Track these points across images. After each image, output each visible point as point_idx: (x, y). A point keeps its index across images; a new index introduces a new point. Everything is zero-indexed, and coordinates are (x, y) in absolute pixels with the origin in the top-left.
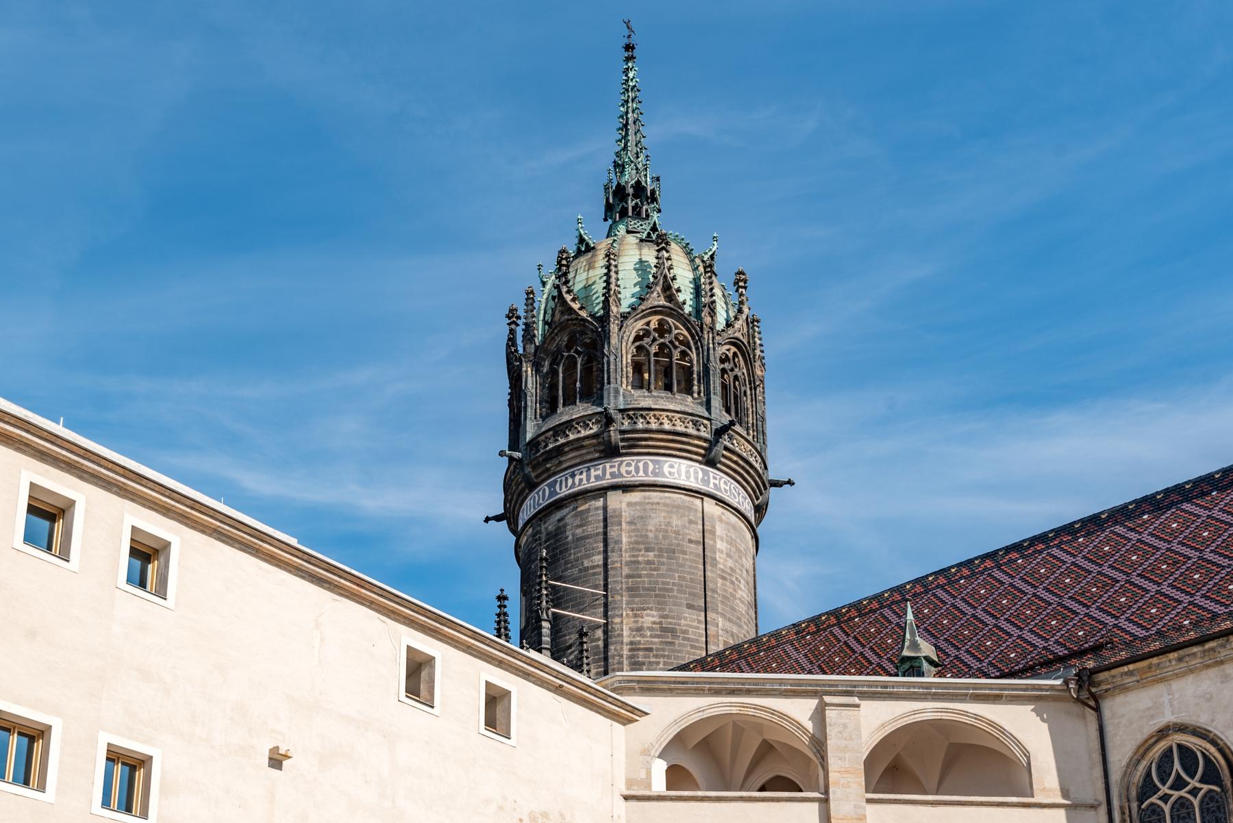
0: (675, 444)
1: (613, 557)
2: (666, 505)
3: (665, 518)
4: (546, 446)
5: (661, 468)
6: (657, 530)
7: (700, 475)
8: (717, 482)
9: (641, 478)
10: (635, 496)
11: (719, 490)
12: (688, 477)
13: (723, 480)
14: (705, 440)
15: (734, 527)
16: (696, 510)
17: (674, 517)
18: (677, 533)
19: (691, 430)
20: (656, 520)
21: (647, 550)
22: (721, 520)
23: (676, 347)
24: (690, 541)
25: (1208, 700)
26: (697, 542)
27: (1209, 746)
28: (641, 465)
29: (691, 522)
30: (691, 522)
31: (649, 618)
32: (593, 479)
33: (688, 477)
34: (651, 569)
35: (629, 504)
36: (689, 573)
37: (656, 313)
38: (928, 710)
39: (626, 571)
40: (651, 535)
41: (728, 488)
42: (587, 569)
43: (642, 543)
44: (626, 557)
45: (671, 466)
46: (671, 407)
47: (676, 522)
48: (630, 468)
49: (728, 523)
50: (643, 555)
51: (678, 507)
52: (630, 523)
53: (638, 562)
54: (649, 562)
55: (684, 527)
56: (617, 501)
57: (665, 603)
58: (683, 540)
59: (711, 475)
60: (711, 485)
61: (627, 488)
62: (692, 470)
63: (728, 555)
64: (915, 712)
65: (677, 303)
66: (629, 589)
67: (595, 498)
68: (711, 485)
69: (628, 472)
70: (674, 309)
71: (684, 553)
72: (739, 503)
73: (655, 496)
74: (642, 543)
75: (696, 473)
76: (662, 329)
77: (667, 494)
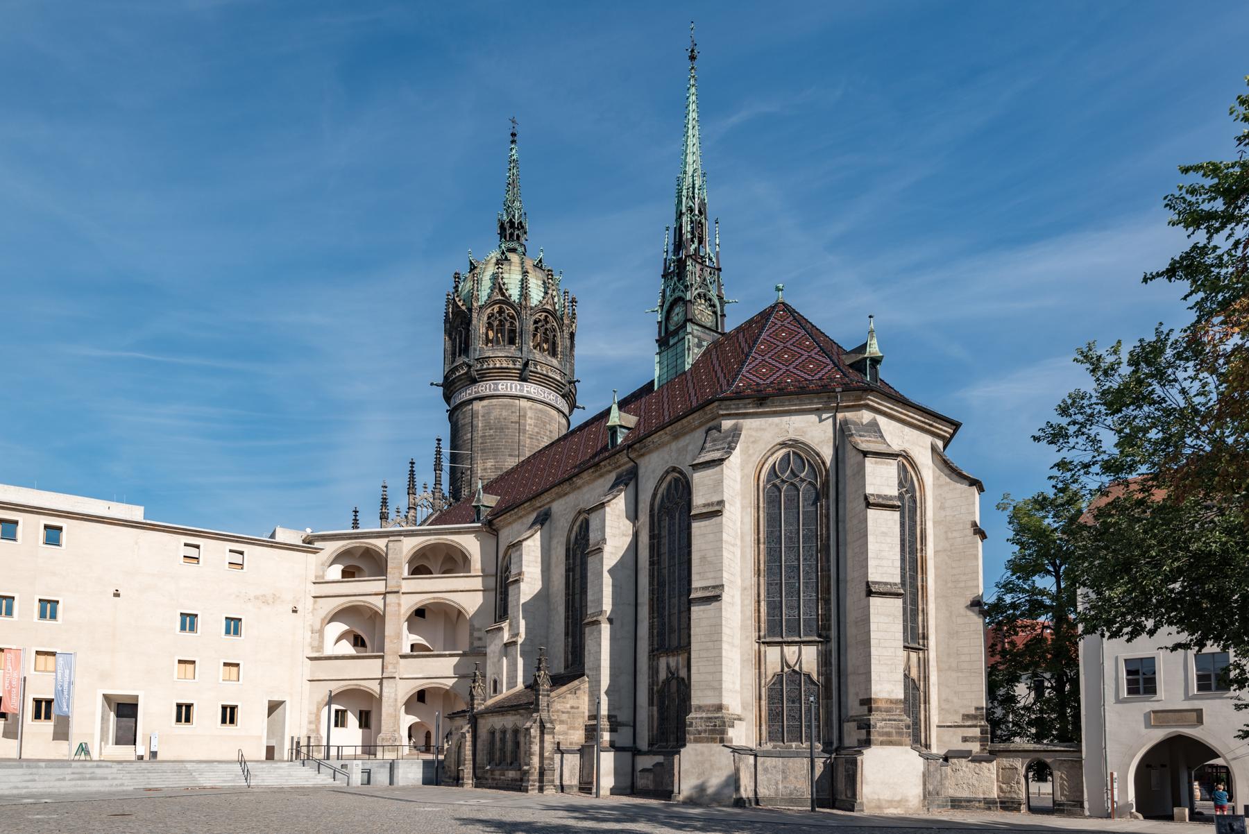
0: (503, 373)
1: (475, 434)
2: (500, 405)
5: (497, 387)
6: (495, 419)
7: (518, 387)
9: (488, 393)
10: (485, 402)
12: (511, 389)
14: (518, 369)
16: (516, 406)
18: (505, 419)
19: (511, 366)
20: (495, 413)
21: (490, 429)
23: (507, 320)
24: (512, 422)
26: (516, 422)
28: (488, 386)
29: (512, 412)
30: (512, 412)
31: (490, 463)
33: (511, 389)
35: (483, 407)
37: (497, 303)
38: (432, 539)
39: (480, 441)
40: (492, 421)
43: (488, 426)
44: (480, 433)
45: (503, 385)
46: (500, 355)
47: (504, 413)
48: (484, 388)
51: (506, 405)
52: (483, 416)
53: (485, 436)
54: (490, 436)
55: (509, 415)
56: (478, 406)
57: (497, 455)
61: (481, 399)
64: (427, 541)
65: (506, 297)
66: (481, 450)
67: (469, 405)
70: (506, 301)
71: (508, 429)
73: (494, 401)
74: (488, 426)
75: (516, 386)
76: (501, 312)
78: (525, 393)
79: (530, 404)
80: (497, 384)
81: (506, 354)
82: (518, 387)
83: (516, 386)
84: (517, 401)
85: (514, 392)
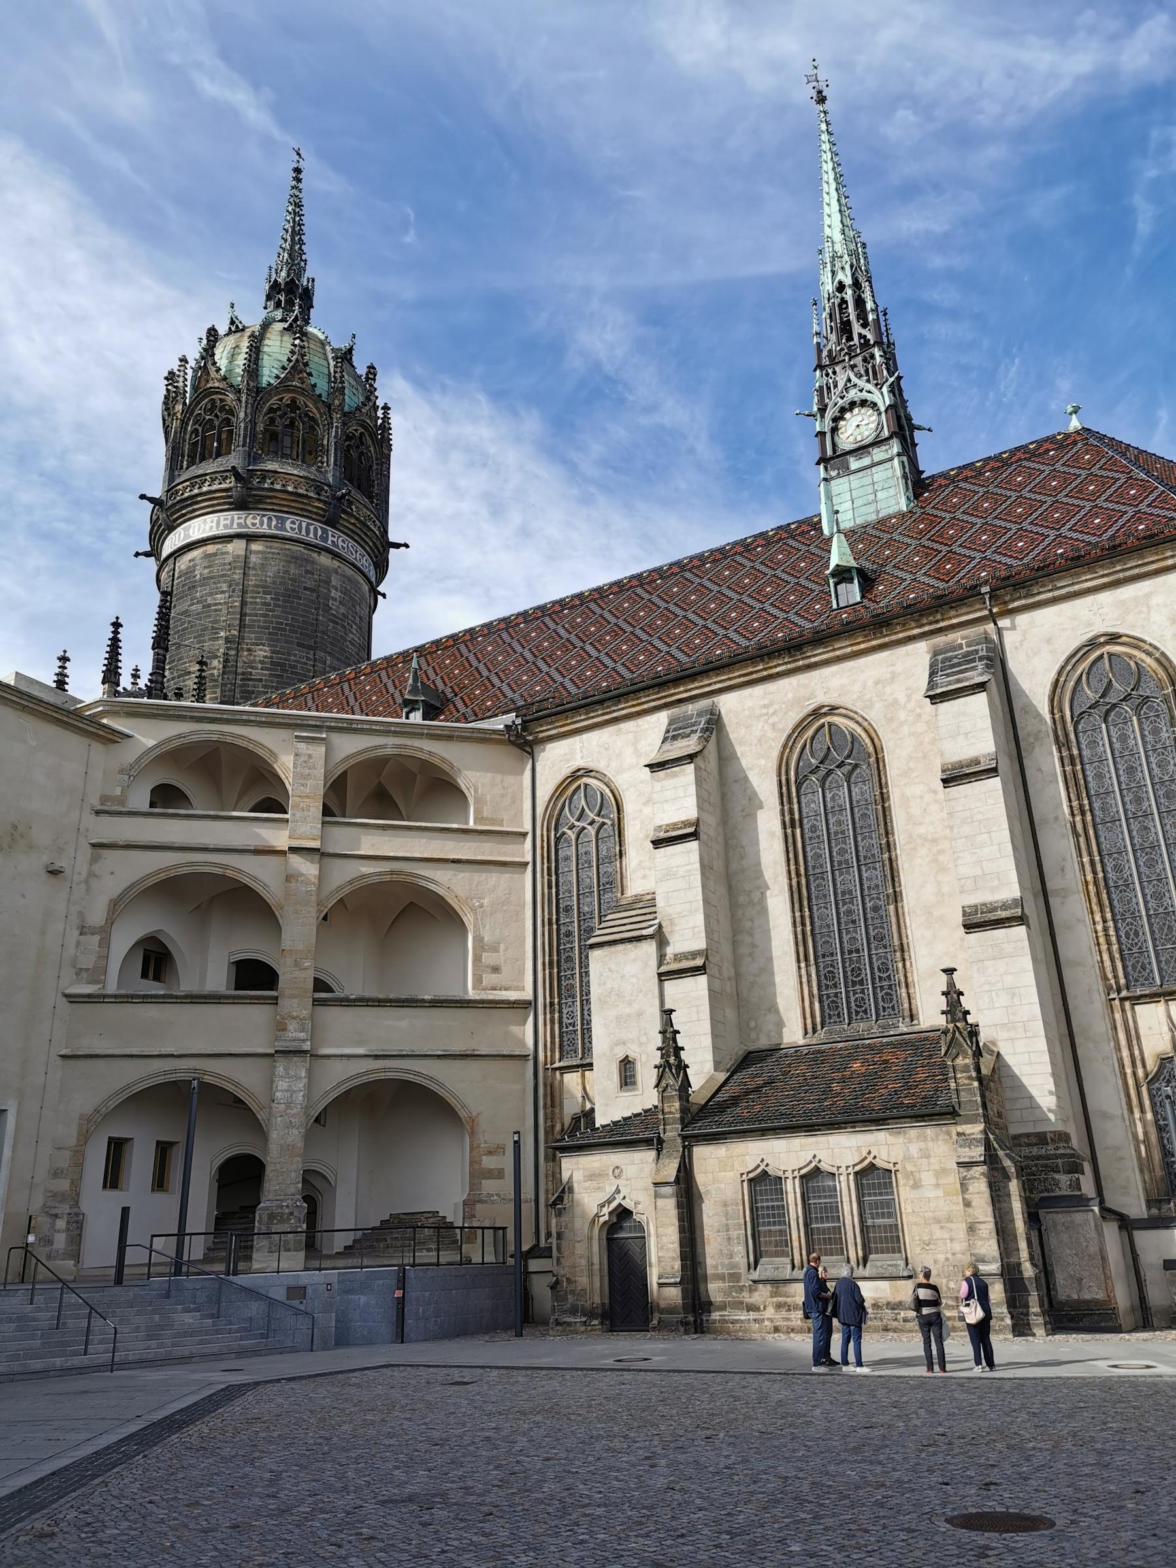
3: (283, 566)
4: (182, 494)
5: (283, 523)
7: (320, 533)
8: (335, 540)
11: (337, 546)
12: (308, 533)
13: (341, 539)
15: (350, 579)
17: (292, 565)
19: (311, 494)
22: (337, 573)
24: (306, 588)
25: (607, 749)
27: (605, 787)
30: (307, 572)
32: (221, 527)
33: (308, 533)
34: (267, 610)
36: (302, 616)
41: (345, 546)
42: (209, 606)
49: (344, 576)
50: (260, 597)
51: (297, 558)
55: (300, 575)
58: (299, 587)
59: (330, 533)
60: (329, 542)
62: (312, 528)
63: (341, 603)
68: (329, 542)
69: (254, 525)
72: (356, 559)
75: (316, 530)
77: (287, 546)
78: (329, 544)
79: (336, 564)
80: (282, 521)
81: (306, 474)
82: (320, 533)
83: (316, 530)
84: (315, 555)
85: (311, 538)
